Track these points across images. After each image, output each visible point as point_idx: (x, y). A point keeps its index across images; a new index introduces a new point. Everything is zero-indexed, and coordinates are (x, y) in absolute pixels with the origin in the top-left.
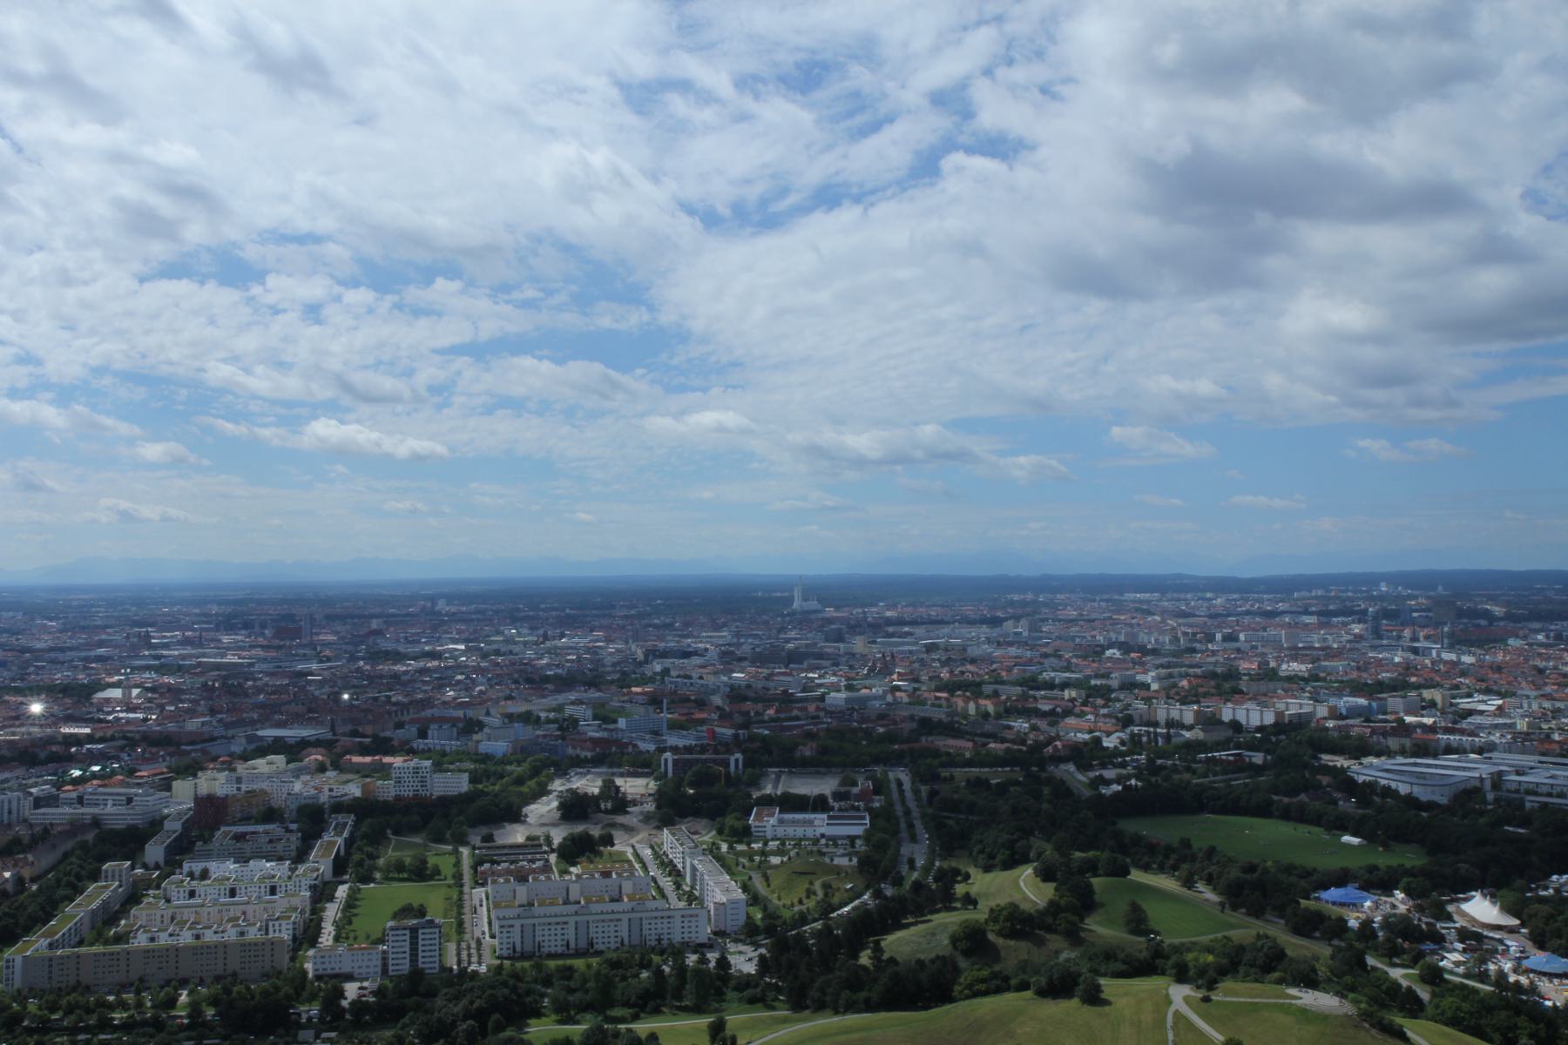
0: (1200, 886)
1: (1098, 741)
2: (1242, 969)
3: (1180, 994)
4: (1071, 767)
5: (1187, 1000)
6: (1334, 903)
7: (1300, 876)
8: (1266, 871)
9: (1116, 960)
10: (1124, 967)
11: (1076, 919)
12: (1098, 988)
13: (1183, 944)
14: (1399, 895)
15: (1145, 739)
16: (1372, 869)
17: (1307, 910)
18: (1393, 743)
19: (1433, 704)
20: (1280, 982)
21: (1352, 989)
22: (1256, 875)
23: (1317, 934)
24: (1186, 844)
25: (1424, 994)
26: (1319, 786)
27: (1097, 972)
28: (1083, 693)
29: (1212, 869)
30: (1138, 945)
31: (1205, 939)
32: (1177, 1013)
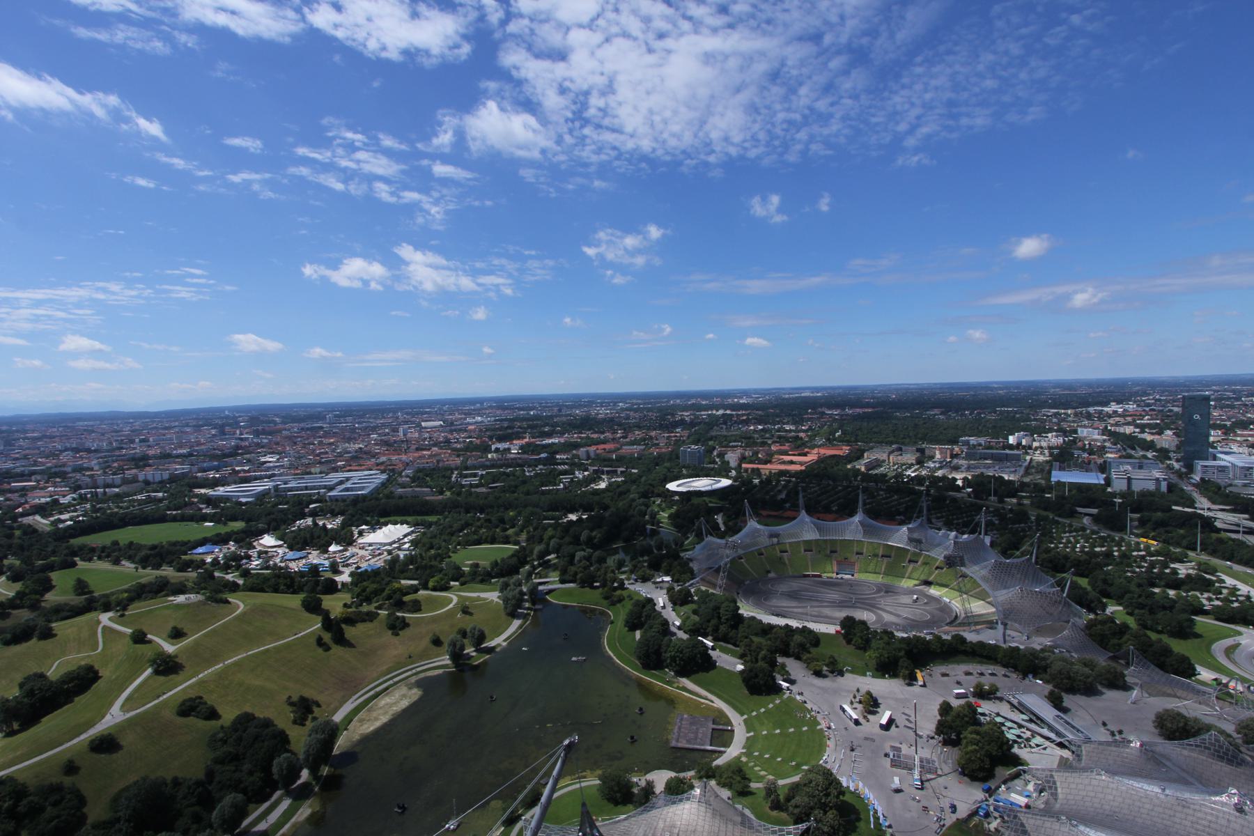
0: (123, 562)
1: (56, 502)
2: (143, 596)
3: (105, 618)
4: (38, 518)
5: (110, 619)
6: (200, 554)
7: (182, 546)
8: (163, 547)
9: (63, 611)
10: (69, 614)
11: (38, 596)
12: (51, 629)
13: (112, 592)
14: (232, 543)
15: (89, 496)
16: (218, 535)
17: (184, 560)
18: (230, 479)
19: (249, 461)
20: (168, 595)
21: (205, 588)
22: (157, 550)
23: (190, 570)
24: (116, 543)
25: (241, 582)
26: (193, 503)
27: (50, 621)
28: (46, 477)
29: (131, 552)
30: (79, 600)
31: (126, 587)
32: (105, 628)
